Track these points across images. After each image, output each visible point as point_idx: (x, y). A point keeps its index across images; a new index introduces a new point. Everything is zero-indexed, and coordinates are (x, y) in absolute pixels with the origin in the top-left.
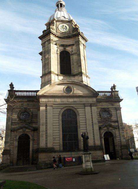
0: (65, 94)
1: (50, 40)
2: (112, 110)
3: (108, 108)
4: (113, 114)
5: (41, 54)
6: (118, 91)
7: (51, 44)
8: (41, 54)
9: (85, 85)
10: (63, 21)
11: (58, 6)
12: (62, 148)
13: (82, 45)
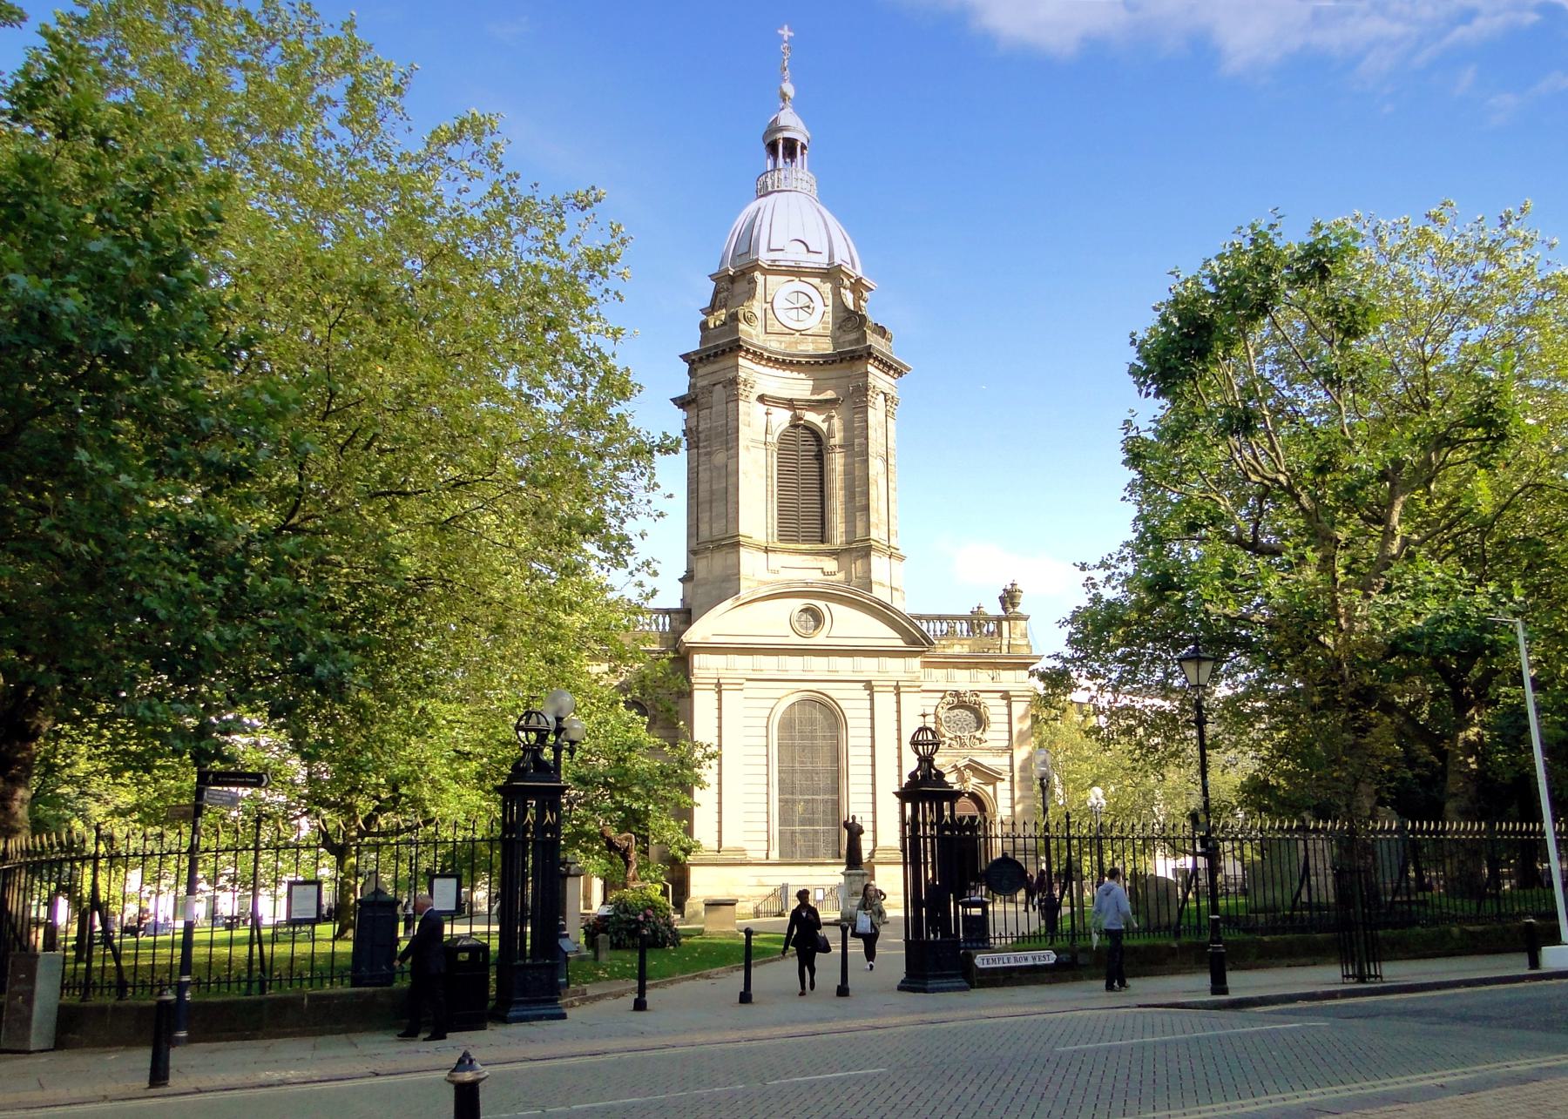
0: (795, 640)
1: (734, 382)
2: (988, 702)
3: (975, 693)
4: (992, 719)
5: (681, 402)
6: (1026, 619)
7: (741, 403)
8: (681, 402)
9: (880, 603)
10: (796, 272)
11: (772, 148)
12: (775, 855)
13: (882, 396)
